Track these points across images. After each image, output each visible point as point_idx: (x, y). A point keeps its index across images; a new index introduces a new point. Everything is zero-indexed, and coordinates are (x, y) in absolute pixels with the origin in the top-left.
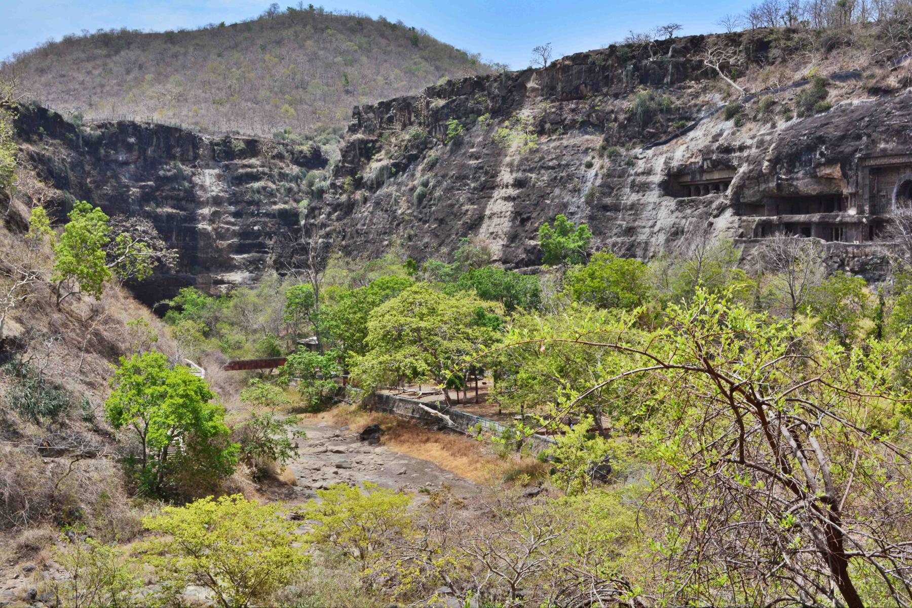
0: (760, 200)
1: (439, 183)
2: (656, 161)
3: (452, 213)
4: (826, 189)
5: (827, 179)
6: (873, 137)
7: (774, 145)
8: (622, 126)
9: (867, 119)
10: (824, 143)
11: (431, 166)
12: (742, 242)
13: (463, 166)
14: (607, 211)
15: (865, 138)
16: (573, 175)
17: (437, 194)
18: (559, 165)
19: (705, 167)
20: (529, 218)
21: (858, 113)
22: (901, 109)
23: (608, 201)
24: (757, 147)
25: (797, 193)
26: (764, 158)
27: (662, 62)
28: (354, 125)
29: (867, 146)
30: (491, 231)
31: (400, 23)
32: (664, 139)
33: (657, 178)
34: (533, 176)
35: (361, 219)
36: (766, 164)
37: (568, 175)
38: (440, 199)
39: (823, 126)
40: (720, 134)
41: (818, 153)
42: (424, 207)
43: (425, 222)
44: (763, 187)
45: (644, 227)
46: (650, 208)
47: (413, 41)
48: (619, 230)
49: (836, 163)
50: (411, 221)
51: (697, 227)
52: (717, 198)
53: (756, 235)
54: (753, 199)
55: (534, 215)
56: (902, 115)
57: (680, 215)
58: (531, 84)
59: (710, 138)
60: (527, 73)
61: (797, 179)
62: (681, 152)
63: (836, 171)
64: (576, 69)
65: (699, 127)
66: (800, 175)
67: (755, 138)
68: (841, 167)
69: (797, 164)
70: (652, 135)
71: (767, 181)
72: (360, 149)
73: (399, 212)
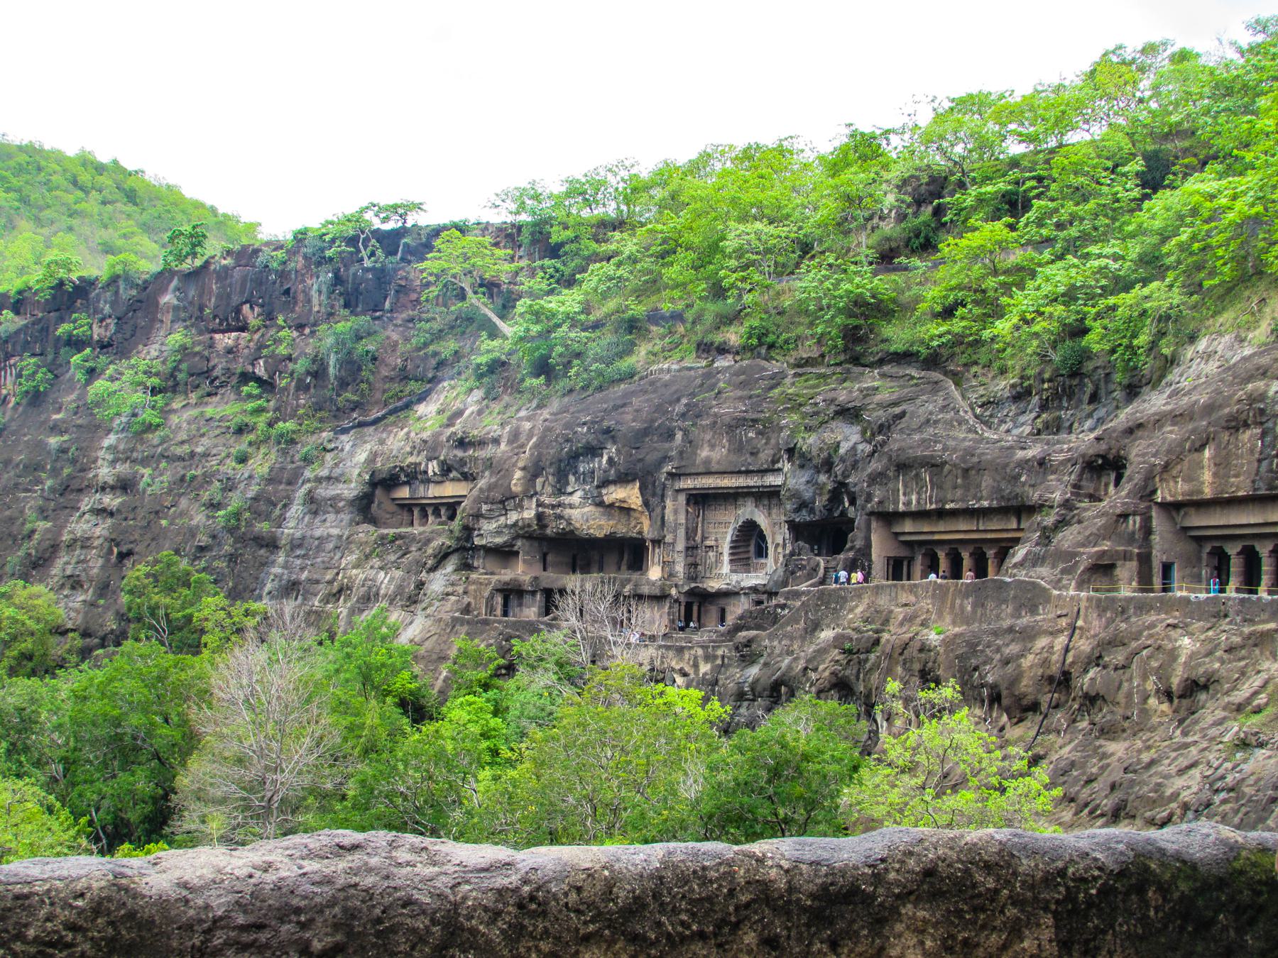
4: (622, 528)
5: (621, 508)
6: (691, 437)
7: (534, 439)
9: (684, 401)
10: (614, 440)
12: (462, 622)
13: (40, 446)
14: (262, 546)
15: (679, 436)
18: (192, 455)
19: (430, 473)
20: (129, 553)
21: (674, 388)
22: (742, 385)
23: (263, 527)
24: (510, 442)
25: (572, 532)
26: (514, 465)
27: (383, 270)
29: (681, 453)
30: (68, 572)
31: (115, 162)
32: (376, 413)
33: (350, 490)
34: (147, 472)
36: (518, 474)
37: (204, 474)
39: (616, 408)
40: (459, 413)
41: (605, 458)
45: (317, 582)
46: (331, 546)
47: (128, 191)
49: (633, 480)
51: (400, 590)
52: (439, 534)
53: (491, 610)
54: (499, 540)
56: (740, 398)
57: (376, 562)
58: (168, 298)
59: (444, 419)
60: (163, 277)
61: (571, 506)
62: (396, 444)
63: (630, 495)
64: (237, 273)
65: (434, 396)
66: (576, 499)
67: (513, 426)
68: (640, 489)
69: (572, 478)
70: (356, 406)
71: (519, 507)
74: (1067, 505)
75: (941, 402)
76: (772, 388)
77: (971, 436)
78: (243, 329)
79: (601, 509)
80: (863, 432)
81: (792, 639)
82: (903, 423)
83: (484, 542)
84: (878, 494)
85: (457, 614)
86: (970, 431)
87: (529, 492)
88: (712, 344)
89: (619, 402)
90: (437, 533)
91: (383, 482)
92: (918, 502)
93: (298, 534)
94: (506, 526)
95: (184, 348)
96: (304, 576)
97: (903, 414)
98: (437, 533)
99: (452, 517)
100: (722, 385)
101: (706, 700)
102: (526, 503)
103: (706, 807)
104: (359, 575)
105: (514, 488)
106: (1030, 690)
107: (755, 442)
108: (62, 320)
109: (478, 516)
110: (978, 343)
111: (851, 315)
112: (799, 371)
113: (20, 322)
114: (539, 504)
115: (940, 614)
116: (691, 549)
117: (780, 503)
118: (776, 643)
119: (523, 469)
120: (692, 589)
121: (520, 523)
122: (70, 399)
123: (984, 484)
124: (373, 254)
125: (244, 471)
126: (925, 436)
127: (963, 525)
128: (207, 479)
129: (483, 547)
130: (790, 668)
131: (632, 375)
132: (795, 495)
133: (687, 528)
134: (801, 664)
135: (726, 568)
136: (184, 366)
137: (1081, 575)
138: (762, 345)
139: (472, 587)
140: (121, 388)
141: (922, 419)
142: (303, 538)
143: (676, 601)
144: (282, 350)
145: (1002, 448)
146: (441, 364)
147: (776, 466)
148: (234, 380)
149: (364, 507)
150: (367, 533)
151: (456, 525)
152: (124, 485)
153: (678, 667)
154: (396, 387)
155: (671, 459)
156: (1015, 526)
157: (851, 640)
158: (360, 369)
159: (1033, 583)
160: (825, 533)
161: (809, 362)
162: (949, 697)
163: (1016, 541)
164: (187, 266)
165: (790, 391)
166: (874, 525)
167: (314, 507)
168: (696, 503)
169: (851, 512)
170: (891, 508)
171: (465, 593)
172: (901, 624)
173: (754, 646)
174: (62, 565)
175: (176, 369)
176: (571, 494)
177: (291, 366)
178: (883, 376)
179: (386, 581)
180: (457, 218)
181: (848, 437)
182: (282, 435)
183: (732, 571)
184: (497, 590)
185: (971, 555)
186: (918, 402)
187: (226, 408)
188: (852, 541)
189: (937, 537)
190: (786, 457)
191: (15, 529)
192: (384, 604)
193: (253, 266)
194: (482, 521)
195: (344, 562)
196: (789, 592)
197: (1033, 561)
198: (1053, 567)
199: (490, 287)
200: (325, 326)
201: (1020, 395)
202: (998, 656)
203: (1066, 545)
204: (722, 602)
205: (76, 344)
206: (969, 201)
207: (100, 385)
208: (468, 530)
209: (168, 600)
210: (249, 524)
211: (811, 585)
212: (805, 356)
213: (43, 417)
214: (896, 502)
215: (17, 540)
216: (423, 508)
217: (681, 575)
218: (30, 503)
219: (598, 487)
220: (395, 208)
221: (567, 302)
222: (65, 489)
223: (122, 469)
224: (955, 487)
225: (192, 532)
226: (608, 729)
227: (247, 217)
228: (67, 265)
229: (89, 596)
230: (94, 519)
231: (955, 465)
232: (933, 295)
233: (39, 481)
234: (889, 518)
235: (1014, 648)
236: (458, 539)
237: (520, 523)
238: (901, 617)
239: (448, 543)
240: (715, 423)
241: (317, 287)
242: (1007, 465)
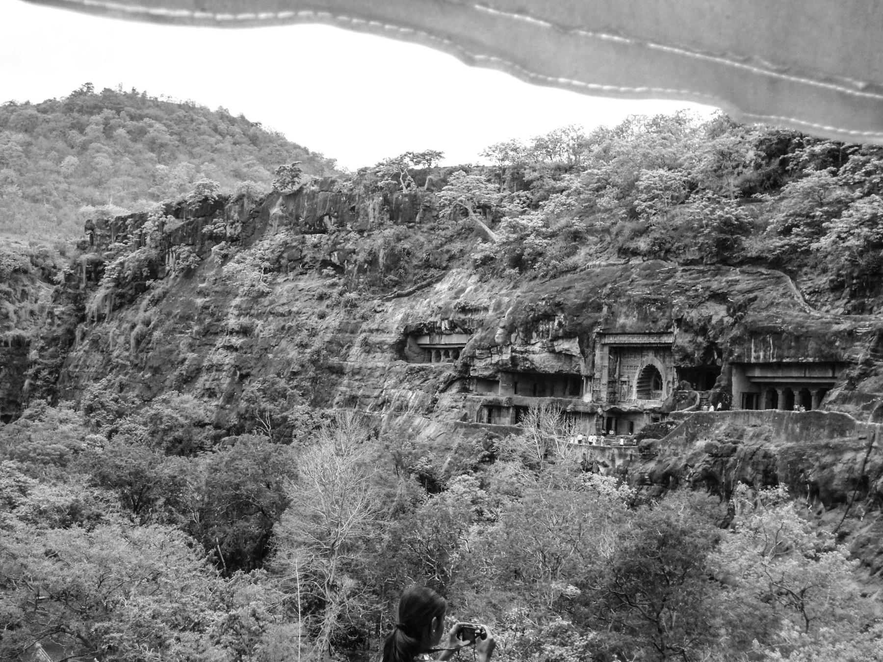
0: (493, 376)
1: (161, 322)
2: (396, 315)
3: (169, 361)
4: (566, 369)
5: (566, 355)
6: (613, 309)
7: (511, 309)
8: (361, 270)
9: (609, 286)
11: (155, 302)
12: (462, 426)
13: (190, 304)
14: (333, 373)
15: (605, 309)
16: (304, 325)
17: (157, 334)
18: (290, 312)
19: (443, 328)
20: (248, 375)
23: (334, 361)
24: (495, 310)
26: (497, 325)
27: (415, 196)
28: (84, 242)
29: (606, 320)
30: (207, 387)
31: (242, 117)
32: (409, 289)
33: (391, 338)
34: (260, 323)
35: (74, 358)
36: (500, 331)
37: (297, 325)
38: (159, 342)
39: (564, 289)
40: (462, 290)
41: (556, 322)
42: (142, 351)
43: (141, 369)
44: (496, 358)
45: (369, 397)
46: (378, 374)
47: (251, 137)
48: (342, 397)
49: (575, 337)
50: (124, 366)
51: (422, 404)
52: (448, 368)
53: (480, 419)
54: (486, 373)
55: (253, 372)
56: (646, 285)
58: (276, 210)
59: (452, 293)
61: (534, 353)
63: (572, 346)
64: (321, 196)
65: (446, 278)
66: (537, 348)
67: (499, 300)
68: (579, 342)
69: (534, 334)
70: (396, 284)
71: (500, 352)
72: (88, 272)
73: (115, 354)
74: (867, 363)
75: (781, 291)
76: (668, 278)
77: (802, 314)
78: (324, 231)
79: (553, 355)
80: (728, 310)
81: (677, 445)
82: (755, 305)
83: (476, 374)
84: (737, 351)
85: (458, 421)
86: (801, 310)
87: (507, 343)
88: (629, 249)
89: (566, 286)
90: (447, 368)
91: (413, 333)
92: (765, 357)
93: (357, 366)
94: (491, 364)
95: (285, 243)
96: (360, 393)
97: (755, 298)
98: (447, 368)
99: (456, 357)
100: (634, 276)
101: (619, 484)
102: (504, 350)
103: (616, 564)
104: (395, 393)
105: (496, 340)
106: (839, 487)
107: (655, 314)
108: (206, 222)
109: (473, 357)
110: (808, 252)
111: (722, 231)
112: (686, 268)
113: (179, 223)
114: (513, 351)
115: (778, 433)
116: (612, 383)
117: (671, 355)
118: (666, 448)
119: (503, 327)
120: (612, 409)
121: (500, 363)
122: (211, 274)
123: (810, 347)
124: (409, 185)
125: (323, 324)
126: (770, 313)
127: (795, 374)
128: (299, 328)
129: (476, 377)
130: (675, 465)
131: (574, 268)
132: (682, 349)
133: (609, 369)
134: (683, 462)
135: (634, 396)
136: (285, 255)
137: (876, 411)
138: (662, 250)
139: (468, 404)
140: (245, 268)
141: (768, 302)
142: (360, 368)
143: (601, 416)
144: (349, 246)
145: (822, 323)
146: (452, 258)
147: (669, 330)
148: (318, 265)
149: (399, 349)
150: (401, 366)
151: (459, 363)
152: (245, 331)
153: (601, 461)
154: (422, 272)
155: (599, 324)
156: (830, 375)
157: (717, 448)
158: (399, 260)
159: (842, 416)
160: (700, 374)
161: (693, 262)
162: (781, 495)
163: (831, 386)
164: (287, 190)
165: (680, 281)
166: (734, 371)
167: (368, 348)
168: (616, 353)
169: (719, 362)
170: (746, 360)
171: (464, 407)
172: (751, 439)
173: (652, 449)
174: (204, 381)
175: (280, 257)
176: (533, 344)
177: (355, 257)
178: (743, 272)
179: (413, 398)
180: (464, 162)
181: (718, 312)
182: (348, 302)
183: (640, 398)
184: (485, 406)
185: (800, 393)
186: (766, 290)
187: (313, 282)
188: (719, 382)
189: (777, 380)
190: (675, 324)
191: (173, 357)
192: (411, 412)
193: (331, 191)
194: (476, 360)
195: (386, 385)
196: (675, 414)
197: (844, 399)
198: (857, 404)
199: (484, 209)
200: (377, 232)
201: (836, 287)
202: (817, 464)
203: (866, 390)
204: (631, 418)
205: (216, 238)
206: (805, 157)
207: (231, 266)
208: (466, 366)
209: (272, 406)
210: (325, 358)
211: (691, 410)
212: (690, 258)
213: (193, 285)
214: (749, 356)
215: (174, 365)
216: (438, 351)
217: (605, 400)
218: (183, 341)
219: (551, 341)
220: (424, 155)
221: (534, 219)
222: (206, 332)
223: (245, 321)
224: (790, 348)
225: (289, 363)
226: (554, 505)
227: (327, 156)
228: (210, 187)
229: (220, 402)
230: (225, 353)
231: (790, 334)
232: (778, 218)
233: (189, 327)
234: (744, 367)
235: (828, 459)
236: (460, 372)
237: (500, 363)
238: (751, 434)
239: (454, 374)
240: (629, 301)
241: (373, 205)
242: (826, 334)
